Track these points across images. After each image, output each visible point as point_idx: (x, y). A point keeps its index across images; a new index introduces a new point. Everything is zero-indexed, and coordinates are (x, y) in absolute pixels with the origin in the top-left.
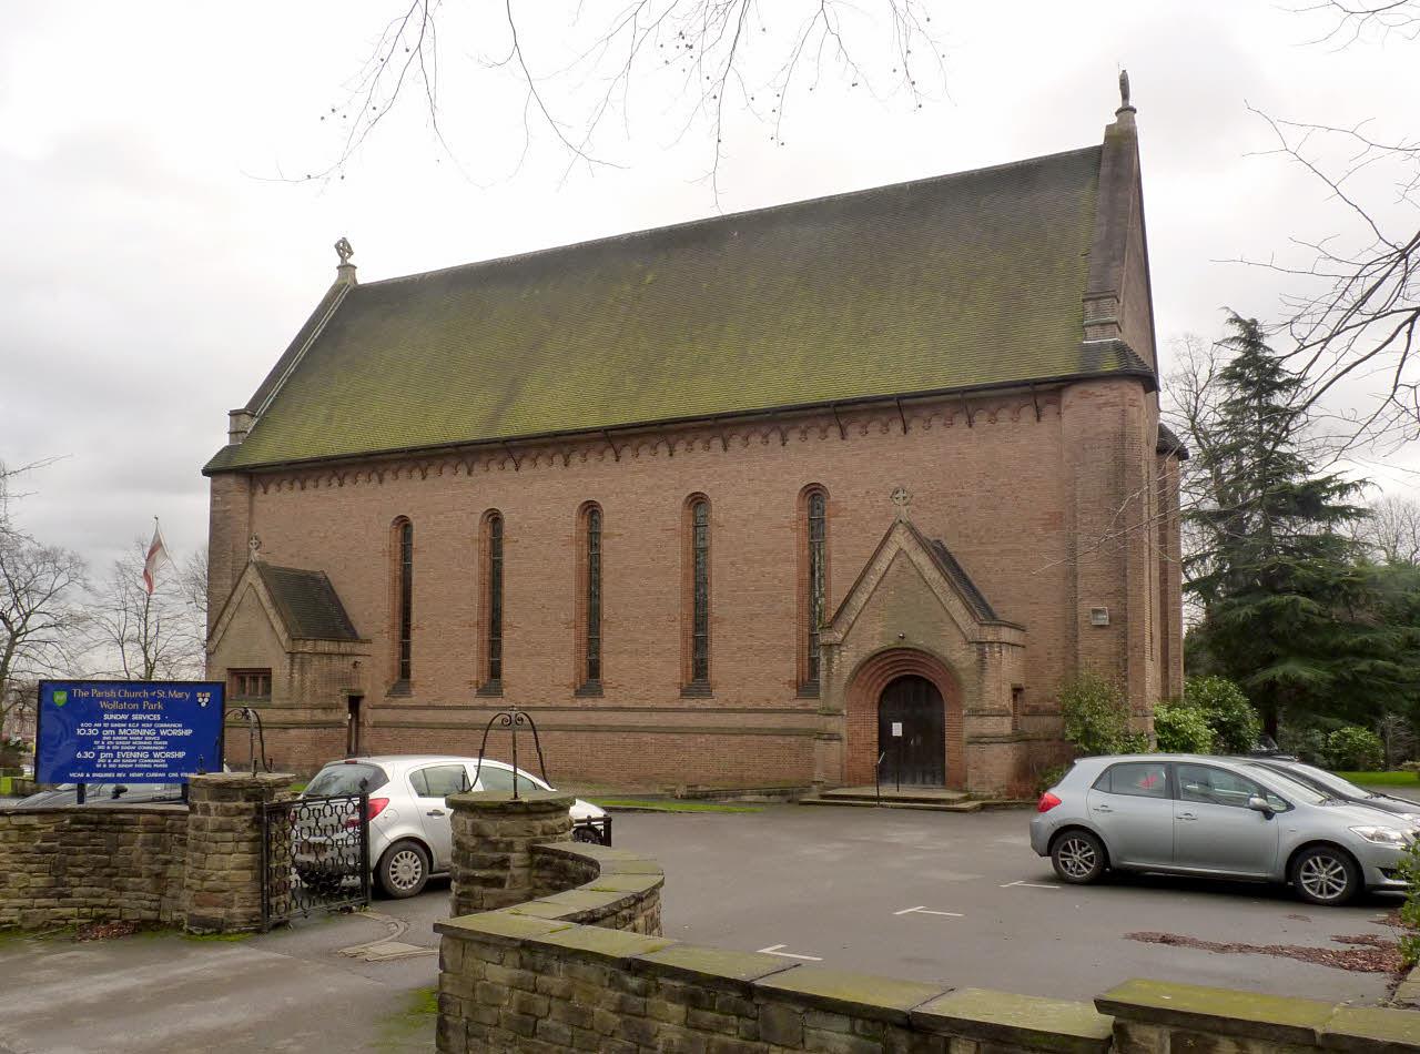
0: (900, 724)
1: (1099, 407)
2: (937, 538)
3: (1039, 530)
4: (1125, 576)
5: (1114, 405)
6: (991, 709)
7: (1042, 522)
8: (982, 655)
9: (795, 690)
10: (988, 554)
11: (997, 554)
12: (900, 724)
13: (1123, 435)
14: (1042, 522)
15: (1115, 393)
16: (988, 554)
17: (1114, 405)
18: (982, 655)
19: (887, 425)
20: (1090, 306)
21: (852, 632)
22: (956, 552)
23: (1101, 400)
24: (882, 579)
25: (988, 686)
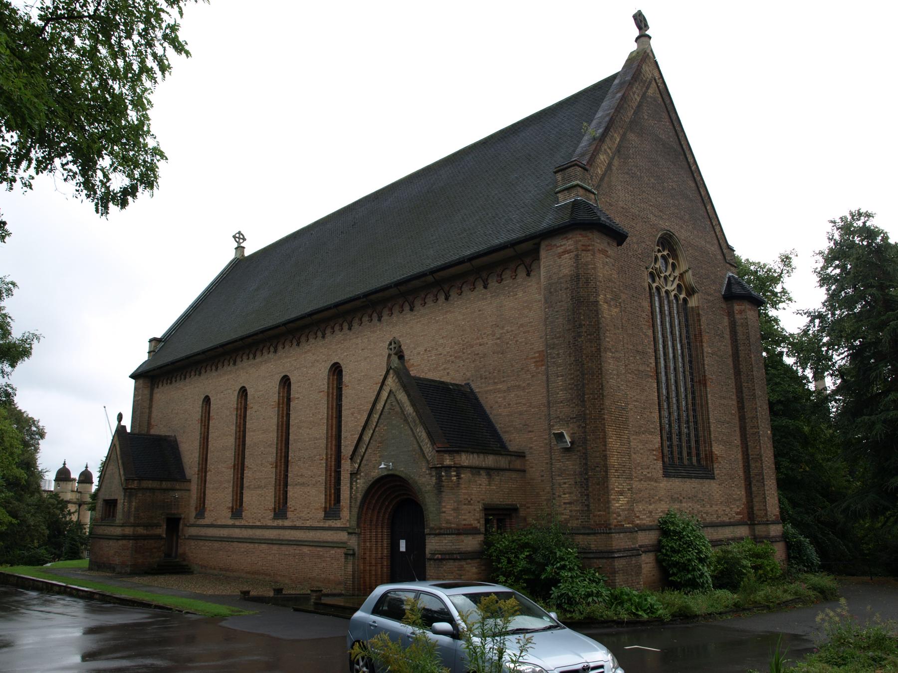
0: (404, 541)
1: (560, 256)
2: (467, 382)
3: (532, 367)
4: (584, 401)
5: (569, 252)
6: (447, 528)
7: (534, 360)
8: (439, 478)
9: (323, 513)
10: (499, 391)
11: (505, 392)
12: (404, 541)
13: (578, 276)
14: (534, 360)
15: (570, 242)
16: (499, 391)
17: (569, 252)
18: (439, 478)
19: (436, 296)
20: (559, 177)
21: (364, 462)
22: (479, 392)
23: (560, 250)
24: (381, 414)
25: (445, 507)
